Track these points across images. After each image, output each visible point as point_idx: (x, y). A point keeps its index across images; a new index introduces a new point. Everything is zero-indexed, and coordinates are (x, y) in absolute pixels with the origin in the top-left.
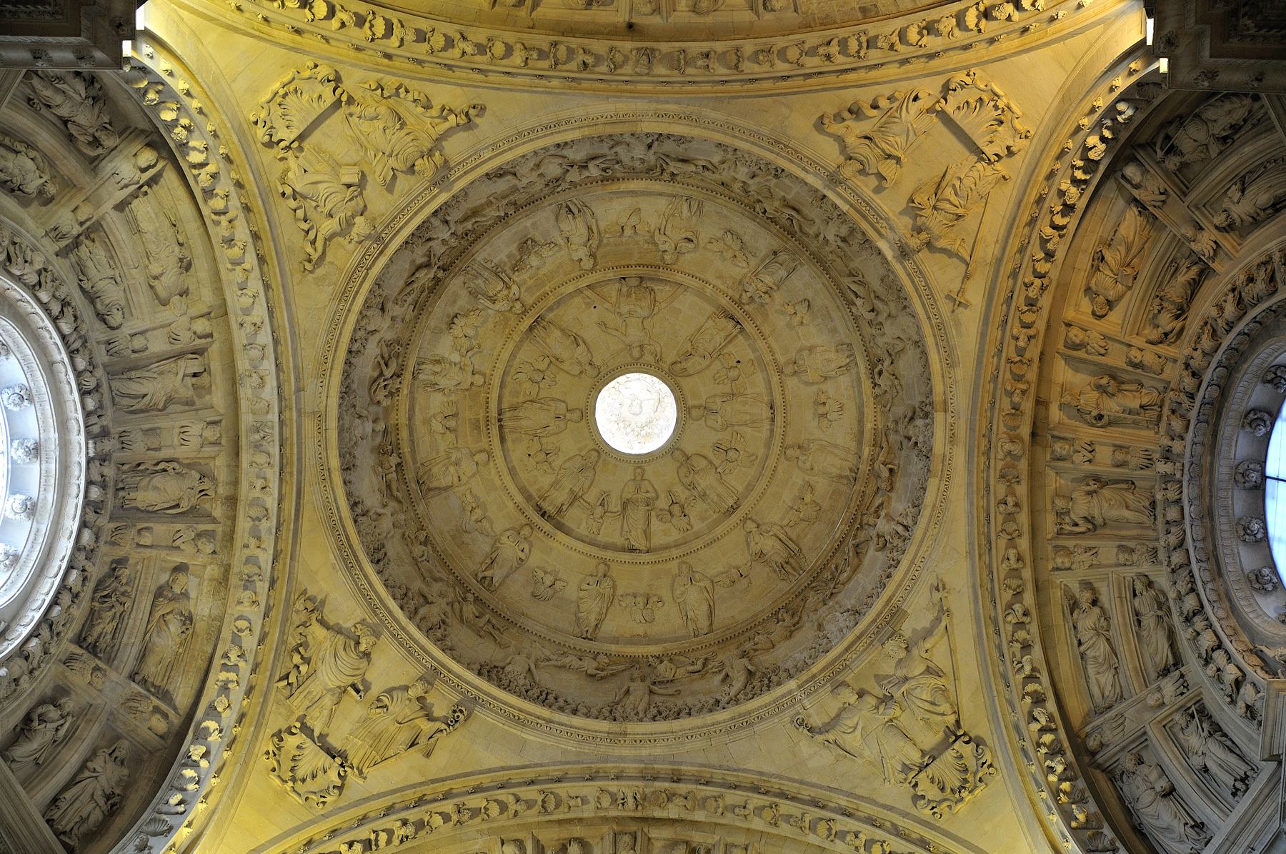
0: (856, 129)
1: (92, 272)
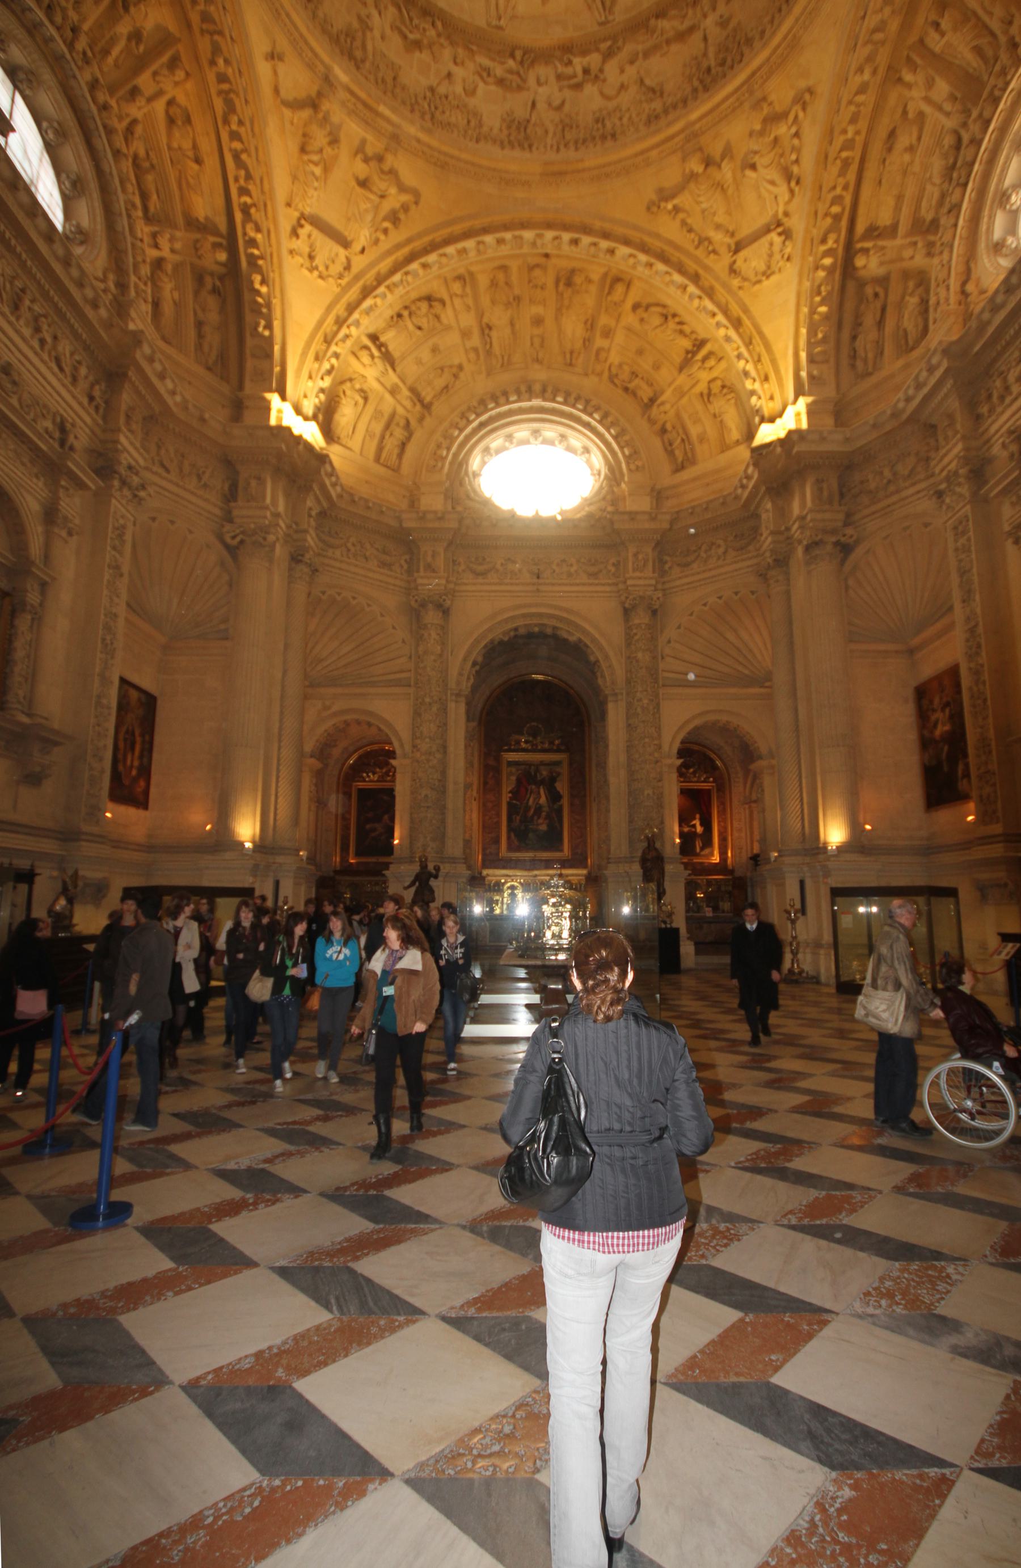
0: (395, 199)
1: (936, 195)
